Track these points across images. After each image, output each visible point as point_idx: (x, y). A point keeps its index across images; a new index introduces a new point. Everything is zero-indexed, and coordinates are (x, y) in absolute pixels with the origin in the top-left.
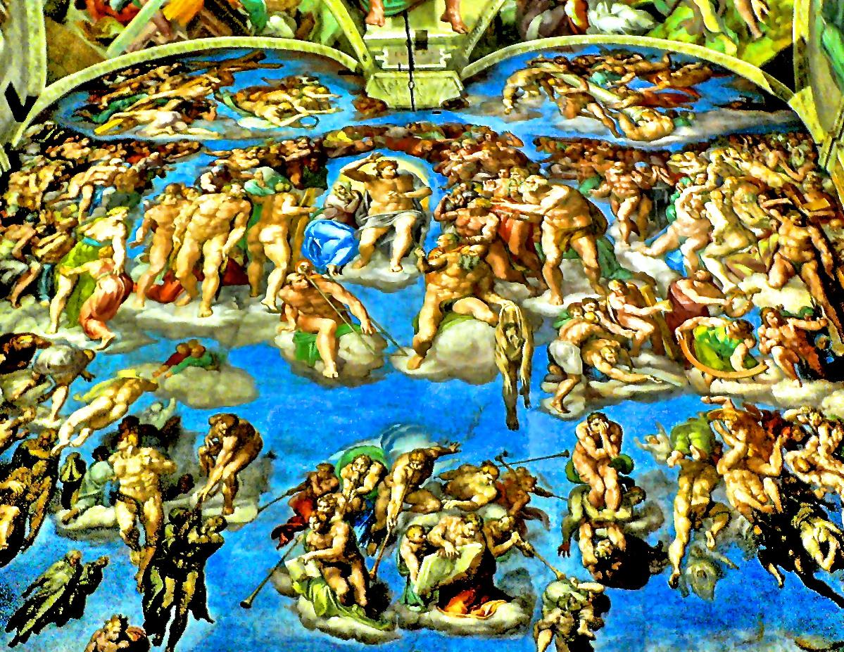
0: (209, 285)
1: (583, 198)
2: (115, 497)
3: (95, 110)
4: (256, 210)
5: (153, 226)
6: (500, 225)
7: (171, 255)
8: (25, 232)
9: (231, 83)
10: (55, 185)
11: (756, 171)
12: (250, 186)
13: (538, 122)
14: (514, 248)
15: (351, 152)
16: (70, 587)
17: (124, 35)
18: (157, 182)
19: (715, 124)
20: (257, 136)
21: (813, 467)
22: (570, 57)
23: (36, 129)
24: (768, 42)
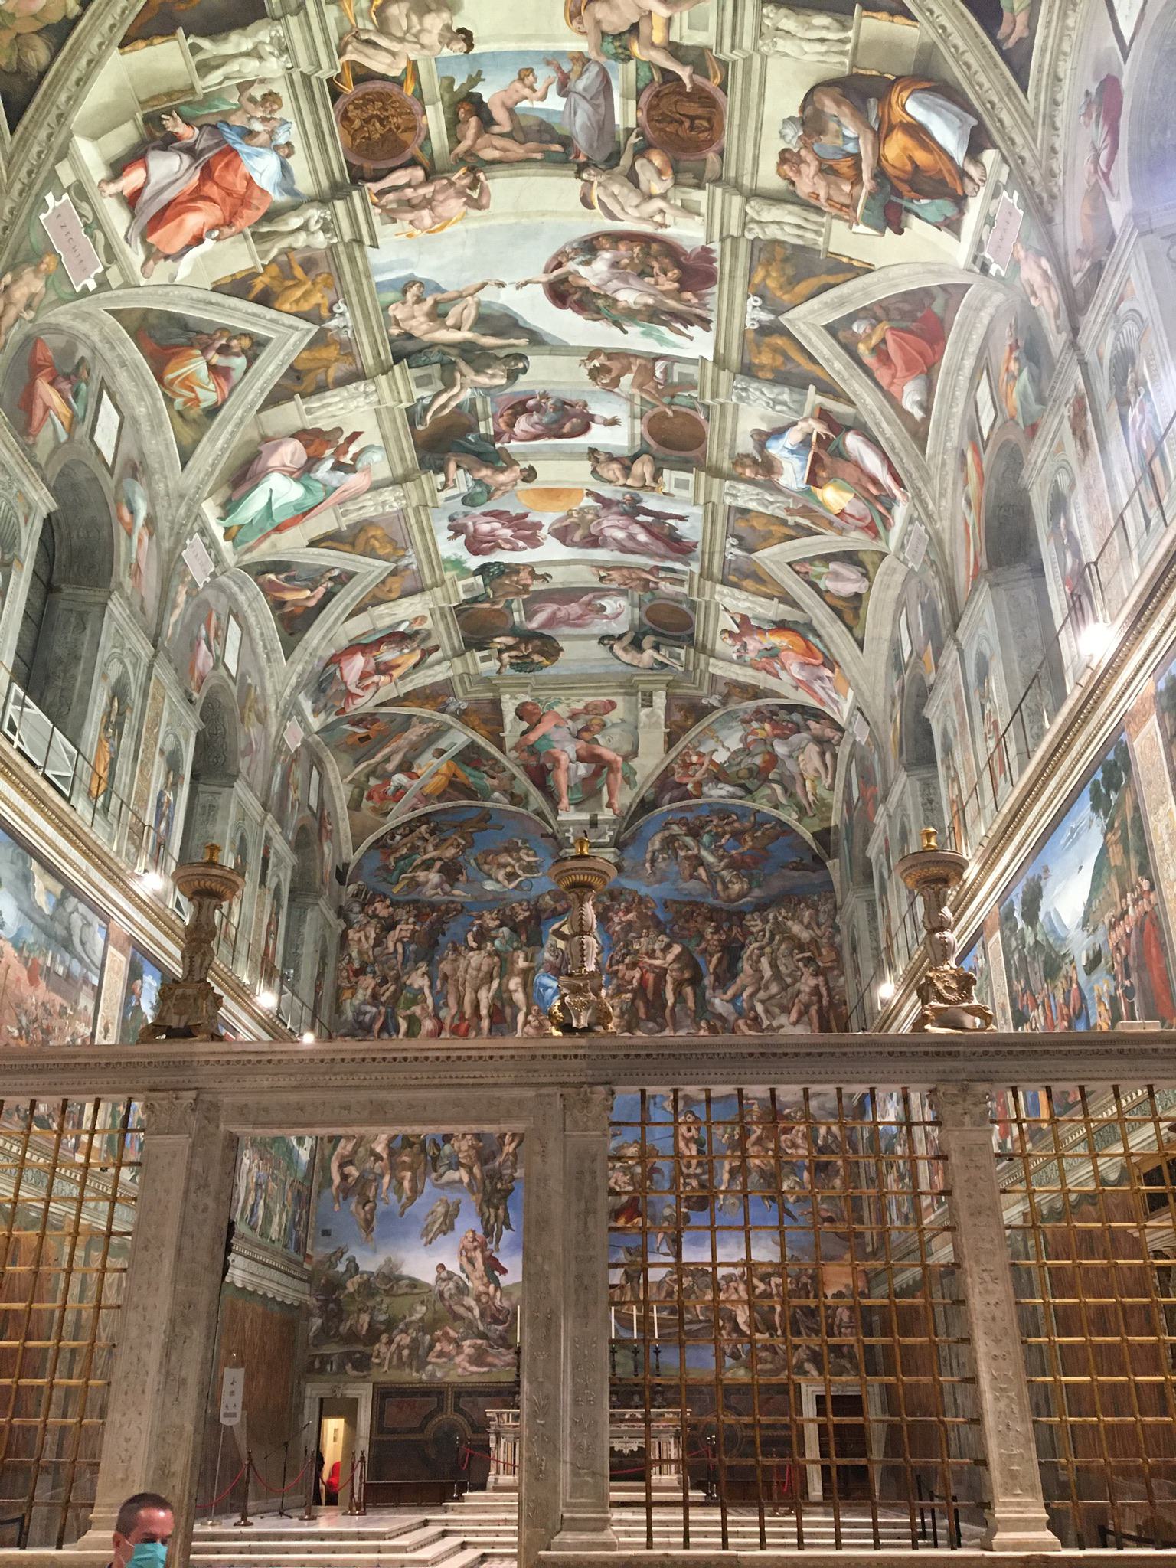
0: (485, 1024)
1: (690, 954)
2: (457, 1165)
3: (386, 868)
4: (503, 966)
5: (445, 978)
6: (642, 977)
7: (460, 1002)
8: (368, 982)
9: (471, 844)
10: (379, 942)
11: (796, 928)
12: (497, 943)
13: (667, 885)
14: (650, 996)
15: (556, 914)
16: (446, 1214)
17: (396, 808)
18: (441, 939)
19: (776, 885)
20: (498, 898)
21: (794, 1145)
22: (689, 816)
23: (352, 888)
24: (816, 820)
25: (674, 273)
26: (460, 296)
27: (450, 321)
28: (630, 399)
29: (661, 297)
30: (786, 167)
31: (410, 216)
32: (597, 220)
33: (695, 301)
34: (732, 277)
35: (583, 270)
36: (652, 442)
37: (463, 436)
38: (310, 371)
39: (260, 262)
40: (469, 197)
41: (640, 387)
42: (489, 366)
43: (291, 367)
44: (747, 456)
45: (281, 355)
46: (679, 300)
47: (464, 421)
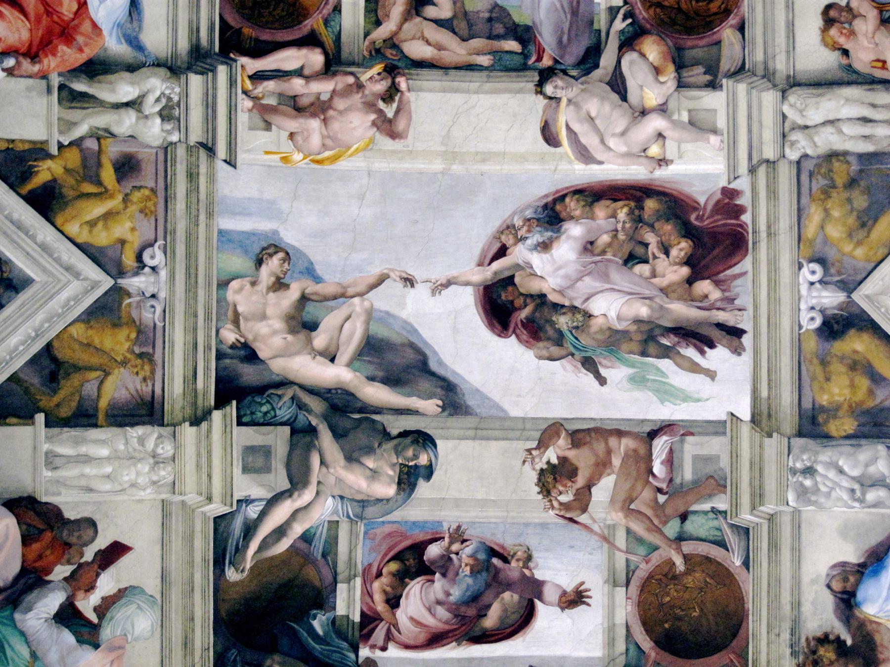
25: (682, 248)
26: (342, 295)
27: (320, 339)
28: (607, 539)
29: (660, 300)
30: (833, 32)
31: (293, 124)
32: (564, 166)
33: (715, 294)
34: (771, 234)
35: (538, 261)
36: (647, 644)
37: (303, 615)
38: (77, 368)
39: (56, 137)
40: (381, 112)
41: (629, 512)
42: (369, 450)
43: (49, 346)
44: (824, 640)
45: (40, 317)
46: (690, 299)
47: (310, 573)
